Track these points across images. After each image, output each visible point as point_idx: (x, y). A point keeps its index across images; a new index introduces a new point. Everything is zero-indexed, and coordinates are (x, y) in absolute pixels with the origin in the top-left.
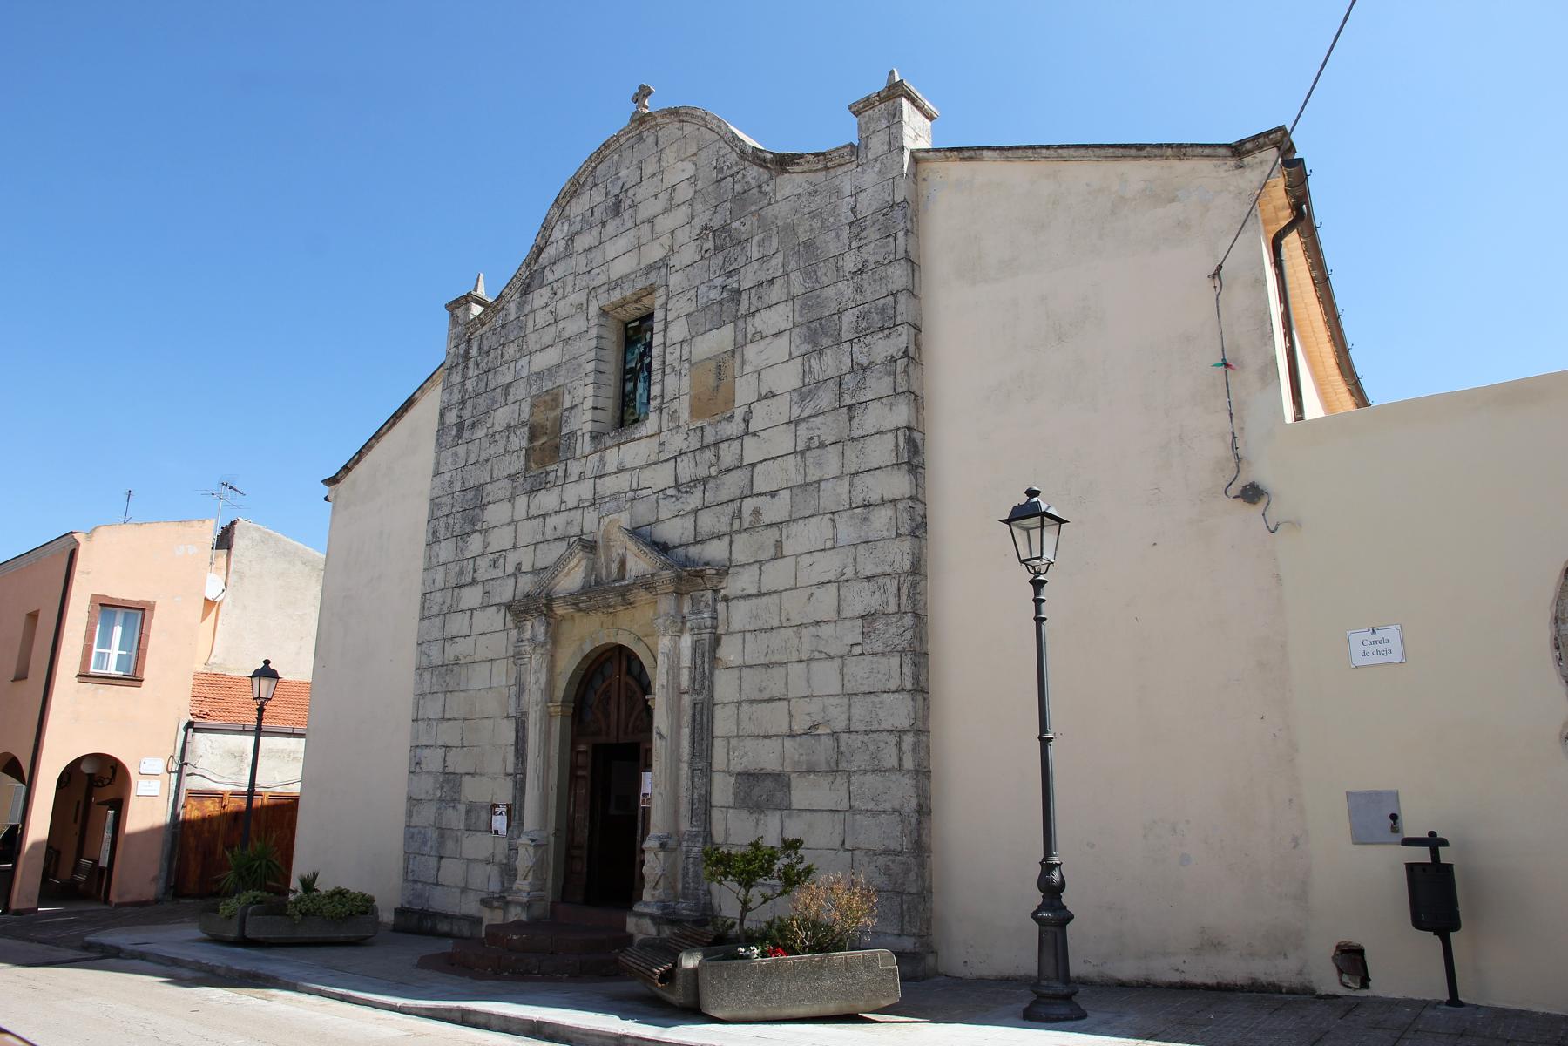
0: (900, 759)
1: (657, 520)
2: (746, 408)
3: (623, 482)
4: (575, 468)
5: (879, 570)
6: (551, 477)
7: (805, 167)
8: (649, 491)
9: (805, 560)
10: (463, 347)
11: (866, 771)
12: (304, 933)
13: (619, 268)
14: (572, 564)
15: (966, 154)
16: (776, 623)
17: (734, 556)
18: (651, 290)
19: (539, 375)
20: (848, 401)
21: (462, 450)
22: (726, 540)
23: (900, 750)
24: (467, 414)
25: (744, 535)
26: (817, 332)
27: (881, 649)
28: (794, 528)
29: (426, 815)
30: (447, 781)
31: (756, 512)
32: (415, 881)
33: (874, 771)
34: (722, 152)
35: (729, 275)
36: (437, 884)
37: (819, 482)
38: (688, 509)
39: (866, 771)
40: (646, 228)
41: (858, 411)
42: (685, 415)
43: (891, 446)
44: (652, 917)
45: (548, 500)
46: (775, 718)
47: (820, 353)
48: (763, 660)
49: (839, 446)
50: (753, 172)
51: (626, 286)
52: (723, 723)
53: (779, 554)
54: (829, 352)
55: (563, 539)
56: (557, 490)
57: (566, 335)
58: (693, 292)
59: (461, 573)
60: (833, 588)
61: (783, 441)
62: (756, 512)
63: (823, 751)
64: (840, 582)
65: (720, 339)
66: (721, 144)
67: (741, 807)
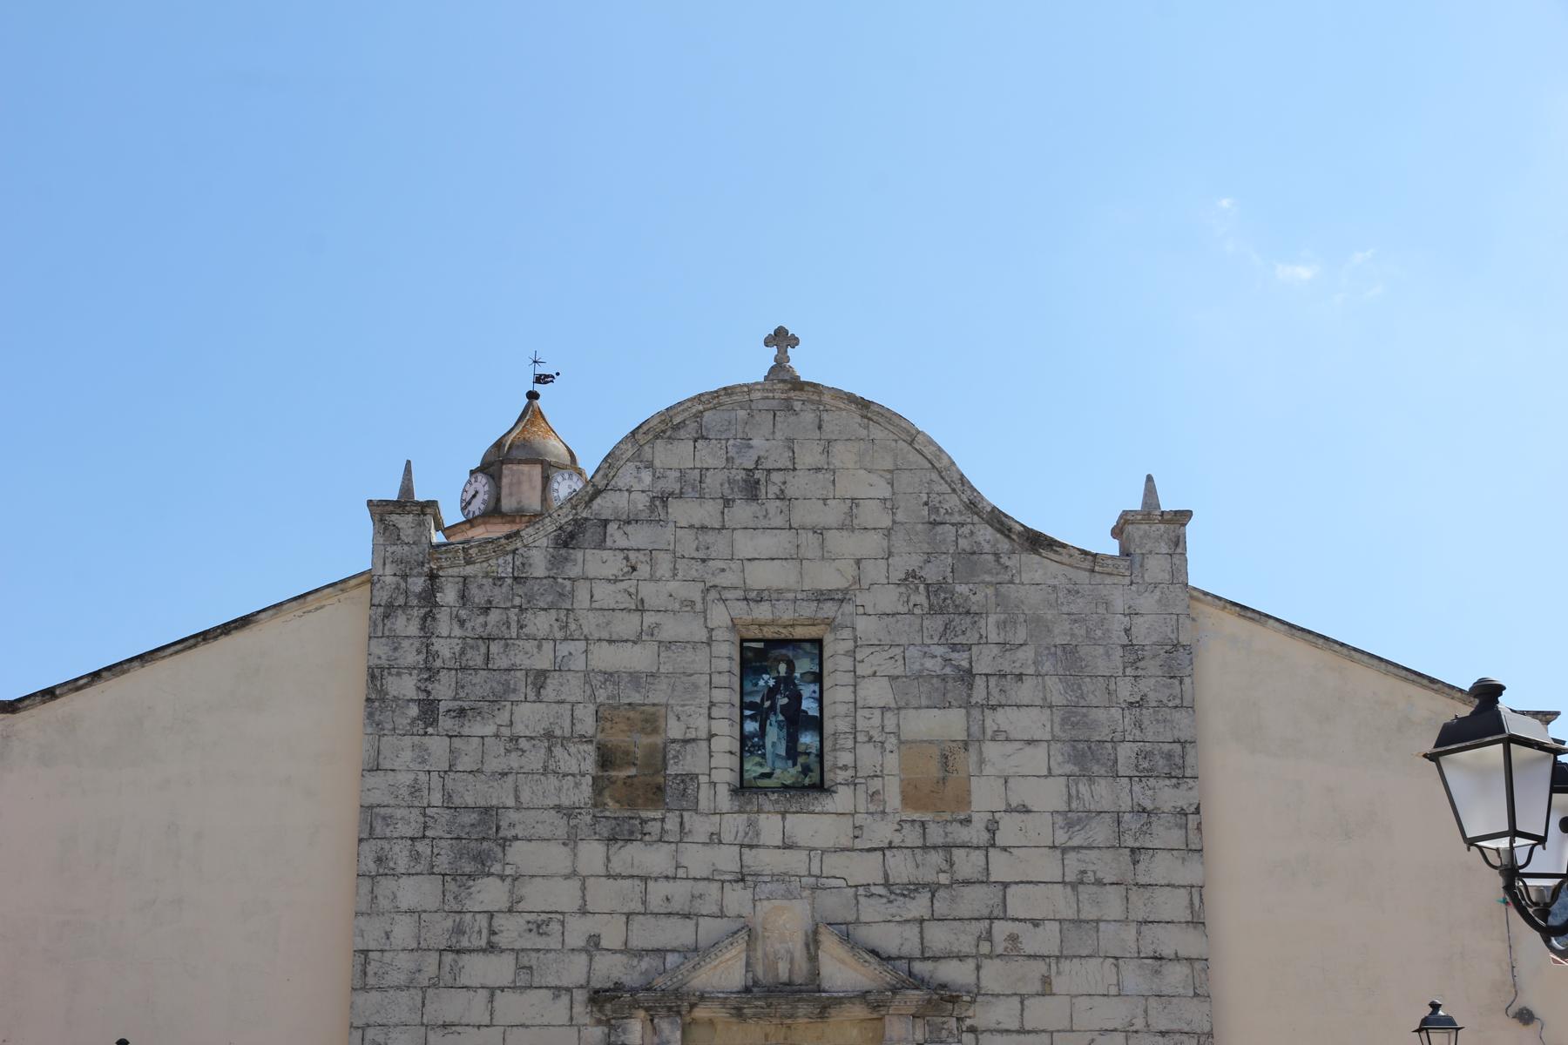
1: (857, 922)
2: (989, 816)
3: (794, 862)
4: (700, 826)
5: (1174, 1027)
6: (654, 828)
7: (1065, 559)
8: (841, 883)
9: (1083, 1003)
10: (418, 584)
13: (763, 576)
14: (728, 956)
15: (1249, 614)
17: (983, 983)
19: (610, 676)
20: (1131, 843)
21: (437, 746)
22: (971, 963)
24: (443, 689)
25: (997, 961)
26: (1085, 755)
28: (1066, 965)
31: (1013, 938)
34: (936, 488)
35: (954, 647)
37: (1097, 921)
38: (910, 916)
40: (808, 539)
42: (893, 800)
43: (1186, 902)
45: (653, 858)
50: (986, 534)
54: (1103, 782)
55: (687, 916)
56: (666, 849)
57: (666, 634)
58: (898, 651)
59: (459, 930)
61: (1048, 867)
62: (1013, 938)
66: (935, 476)
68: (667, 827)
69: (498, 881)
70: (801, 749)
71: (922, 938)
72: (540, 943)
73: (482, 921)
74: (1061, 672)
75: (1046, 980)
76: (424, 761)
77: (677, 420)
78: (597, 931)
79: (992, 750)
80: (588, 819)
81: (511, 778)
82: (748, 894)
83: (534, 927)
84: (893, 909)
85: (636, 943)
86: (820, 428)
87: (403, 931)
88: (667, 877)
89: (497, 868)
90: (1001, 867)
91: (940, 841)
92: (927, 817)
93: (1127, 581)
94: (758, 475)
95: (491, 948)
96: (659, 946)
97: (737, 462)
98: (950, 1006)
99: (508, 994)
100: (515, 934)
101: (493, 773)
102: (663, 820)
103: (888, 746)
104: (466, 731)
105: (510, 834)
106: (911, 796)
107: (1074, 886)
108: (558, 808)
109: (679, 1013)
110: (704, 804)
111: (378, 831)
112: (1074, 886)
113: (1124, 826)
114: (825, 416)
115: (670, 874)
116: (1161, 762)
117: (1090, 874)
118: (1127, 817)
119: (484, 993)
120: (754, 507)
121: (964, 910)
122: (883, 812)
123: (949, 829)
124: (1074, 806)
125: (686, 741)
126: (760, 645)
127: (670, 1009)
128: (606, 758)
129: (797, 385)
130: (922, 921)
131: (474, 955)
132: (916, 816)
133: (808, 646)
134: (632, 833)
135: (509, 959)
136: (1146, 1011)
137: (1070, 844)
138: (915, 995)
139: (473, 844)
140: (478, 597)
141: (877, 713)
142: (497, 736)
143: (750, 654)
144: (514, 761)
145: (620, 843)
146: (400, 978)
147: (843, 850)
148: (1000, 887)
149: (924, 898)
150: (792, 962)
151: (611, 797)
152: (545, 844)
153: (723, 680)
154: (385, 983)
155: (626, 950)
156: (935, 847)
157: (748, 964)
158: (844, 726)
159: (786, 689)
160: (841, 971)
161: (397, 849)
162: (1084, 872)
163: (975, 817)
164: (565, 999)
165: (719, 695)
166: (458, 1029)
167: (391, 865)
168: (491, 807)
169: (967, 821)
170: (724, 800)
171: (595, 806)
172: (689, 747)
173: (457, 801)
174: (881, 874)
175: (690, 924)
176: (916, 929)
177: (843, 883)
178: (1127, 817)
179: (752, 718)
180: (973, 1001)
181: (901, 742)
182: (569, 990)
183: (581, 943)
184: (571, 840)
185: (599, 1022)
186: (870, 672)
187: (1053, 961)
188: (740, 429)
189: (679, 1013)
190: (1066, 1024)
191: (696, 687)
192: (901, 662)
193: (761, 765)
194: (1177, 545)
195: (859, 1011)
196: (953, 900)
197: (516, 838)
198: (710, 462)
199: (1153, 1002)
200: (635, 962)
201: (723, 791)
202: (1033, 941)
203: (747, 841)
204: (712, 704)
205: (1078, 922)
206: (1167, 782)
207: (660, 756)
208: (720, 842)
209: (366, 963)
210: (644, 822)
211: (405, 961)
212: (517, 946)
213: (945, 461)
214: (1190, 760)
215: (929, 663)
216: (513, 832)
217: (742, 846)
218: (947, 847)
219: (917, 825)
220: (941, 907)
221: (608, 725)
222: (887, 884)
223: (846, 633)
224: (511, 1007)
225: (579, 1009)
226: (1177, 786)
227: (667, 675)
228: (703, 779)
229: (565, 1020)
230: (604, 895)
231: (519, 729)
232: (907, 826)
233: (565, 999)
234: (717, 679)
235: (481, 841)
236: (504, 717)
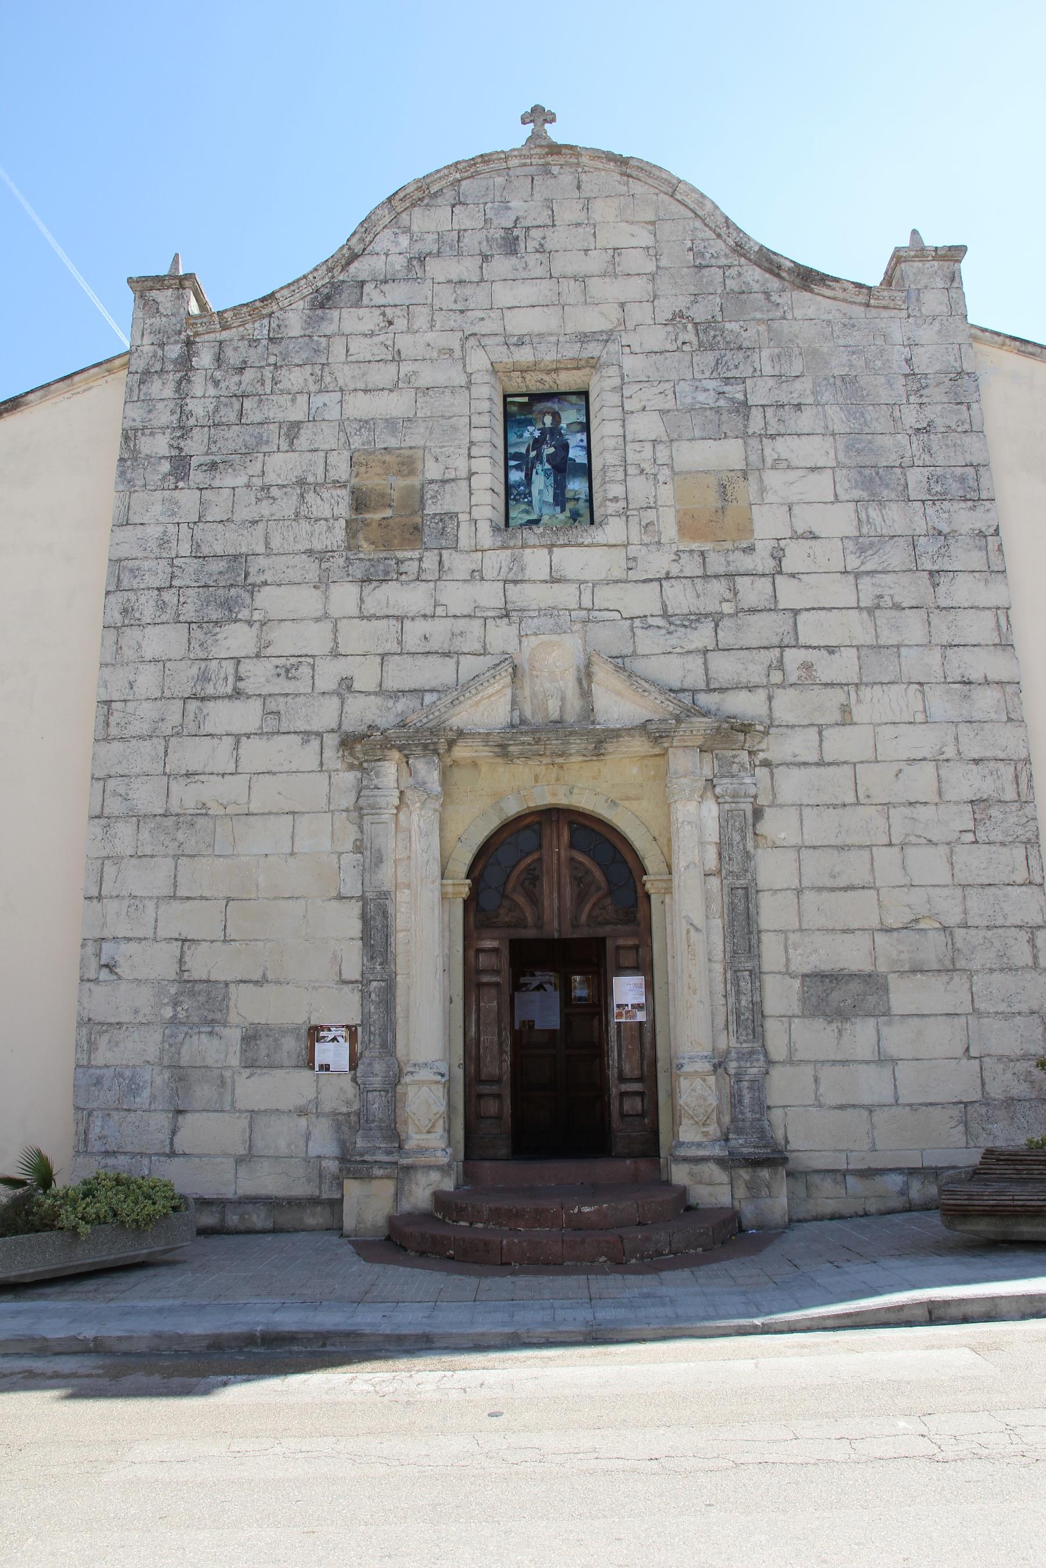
0: (1035, 957)
1: (634, 654)
2: (774, 543)
3: (565, 595)
4: (460, 564)
5: (989, 754)
7: (839, 294)
9: (888, 731)
10: (174, 351)
11: (992, 970)
12: (85, 1257)
13: (521, 323)
14: (490, 690)
15: (1030, 349)
16: (850, 798)
17: (777, 714)
18: (594, 364)
19: (365, 423)
21: (188, 499)
22: (761, 695)
23: (1034, 946)
24: (195, 446)
25: (791, 691)
26: (873, 482)
27: (1000, 838)
28: (866, 693)
29: (138, 1049)
30: (192, 994)
31: (807, 666)
32: (107, 1153)
33: (1002, 970)
34: (700, 235)
35: (727, 380)
36: (173, 1154)
37: (898, 646)
38: (692, 647)
39: (992, 970)
41: (943, 579)
42: (669, 530)
44: (720, 1162)
45: (409, 597)
46: (860, 909)
47: (882, 504)
48: (839, 842)
49: (923, 613)
50: (754, 275)
51: (543, 348)
52: (772, 913)
53: (846, 718)
54: (894, 506)
55: (447, 654)
57: (423, 382)
58: (668, 386)
59: (204, 678)
60: (930, 767)
61: (842, 593)
62: (807, 666)
63: (932, 948)
64: (939, 761)
65: (729, 453)
66: (698, 224)
67: (813, 1016)
68: (424, 566)
69: (246, 627)
70: (569, 495)
71: (706, 670)
72: (290, 687)
73: (229, 667)
74: (841, 400)
75: (845, 710)
76: (174, 514)
77: (434, 189)
78: (349, 674)
79: (773, 479)
80: (341, 561)
81: (261, 526)
82: (514, 630)
83: (282, 671)
84: (673, 640)
85: (391, 683)
86: (579, 187)
87: (147, 680)
88: (425, 616)
89: (244, 614)
90: (789, 594)
91: (722, 570)
92: (707, 546)
93: (904, 314)
94: (516, 232)
95: (237, 694)
96: (417, 686)
97: (495, 222)
98: (741, 737)
99: (255, 741)
100: (263, 680)
101: (243, 522)
102: (420, 560)
103: (661, 478)
104: (217, 483)
105: (259, 580)
106: (689, 526)
107: (871, 611)
108: (310, 552)
109: (435, 751)
110: (464, 542)
111: (125, 584)
112: (871, 611)
113: (920, 549)
114: (583, 177)
115: (428, 613)
116: (955, 486)
117: (887, 598)
118: (922, 540)
119: (230, 740)
120: (514, 260)
121: (753, 641)
122: (659, 543)
123: (731, 558)
124: (865, 530)
125: (444, 482)
126: (525, 399)
127: (425, 747)
128: (360, 502)
129: (555, 149)
130: (706, 652)
131: (219, 702)
132: (694, 546)
133: (573, 399)
134: (387, 573)
135: (256, 705)
136: (957, 739)
137: (863, 569)
138: (701, 723)
139: (220, 592)
140: (233, 358)
141: (648, 446)
142: (248, 486)
143: (514, 409)
144: (265, 509)
145: (375, 584)
146: (145, 728)
147: (617, 582)
148: (790, 614)
149: (706, 628)
150: (563, 699)
151: (366, 539)
152: (295, 587)
153: (485, 420)
154: (127, 733)
155: (381, 692)
156: (716, 576)
157: (514, 703)
158: (612, 458)
159: (552, 439)
160: (617, 704)
161: (143, 599)
162: (881, 597)
163: (759, 545)
164: (315, 743)
165: (479, 435)
166: (202, 778)
167: (137, 615)
168: (241, 555)
169: (750, 549)
170: (486, 536)
171: (349, 548)
172: (447, 486)
173: (205, 550)
174: (659, 606)
175: (451, 662)
176: (700, 660)
177: (617, 615)
178: (922, 540)
179: (517, 467)
180: (766, 733)
181: (674, 473)
182: (319, 735)
183: (332, 686)
184: (323, 583)
185: (351, 767)
186: (639, 406)
187: (852, 689)
188: (498, 194)
189: (435, 751)
190: (869, 755)
191: (455, 429)
192: (671, 396)
193: (527, 512)
194: (953, 280)
195: (639, 745)
196: (739, 628)
197: (265, 583)
198: (468, 224)
199: (963, 729)
200: (390, 703)
201: (484, 528)
202: (828, 669)
203: (511, 577)
204: (472, 443)
205: (877, 648)
206: (963, 505)
207: (418, 499)
208: (482, 579)
209: (109, 712)
210: (399, 562)
211: (148, 710)
212: (265, 691)
213: (709, 207)
214: (984, 483)
215: (701, 397)
216: (262, 578)
217: (505, 582)
218: (730, 576)
219: (696, 555)
220: (726, 637)
221: (363, 469)
222: (665, 615)
223: (613, 371)
224: (257, 753)
225: (329, 753)
226: (973, 508)
227: (424, 419)
228: (463, 517)
229: (315, 766)
230: (356, 636)
231: (271, 478)
232: (685, 557)
233: (315, 743)
234: (476, 420)
235: (229, 588)
236: (255, 468)
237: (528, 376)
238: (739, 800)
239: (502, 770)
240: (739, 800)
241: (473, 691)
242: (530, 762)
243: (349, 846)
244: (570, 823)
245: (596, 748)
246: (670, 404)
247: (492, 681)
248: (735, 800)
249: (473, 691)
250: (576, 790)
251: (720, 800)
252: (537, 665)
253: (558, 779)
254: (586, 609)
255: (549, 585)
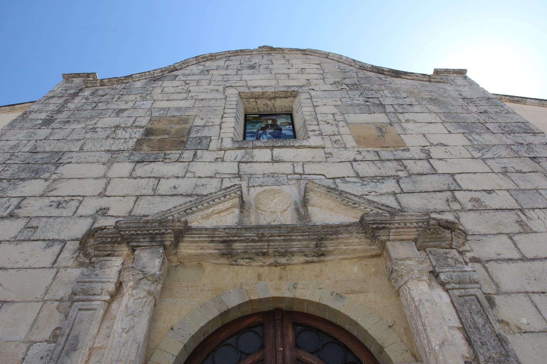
14: (221, 207)
98: (448, 234)
109: (162, 244)
151: (147, 146)
195: (357, 243)
217: (240, 162)
237: (259, 101)
238: (466, 286)
239: (226, 270)
240: (466, 286)
241: (205, 205)
242: (254, 264)
243: (47, 334)
244: (295, 324)
245: (317, 246)
246: (339, 103)
247: (223, 199)
248: (462, 286)
249: (205, 205)
250: (299, 286)
251: (448, 286)
252: (262, 207)
253: (281, 278)
254: (299, 174)
255: (271, 164)
